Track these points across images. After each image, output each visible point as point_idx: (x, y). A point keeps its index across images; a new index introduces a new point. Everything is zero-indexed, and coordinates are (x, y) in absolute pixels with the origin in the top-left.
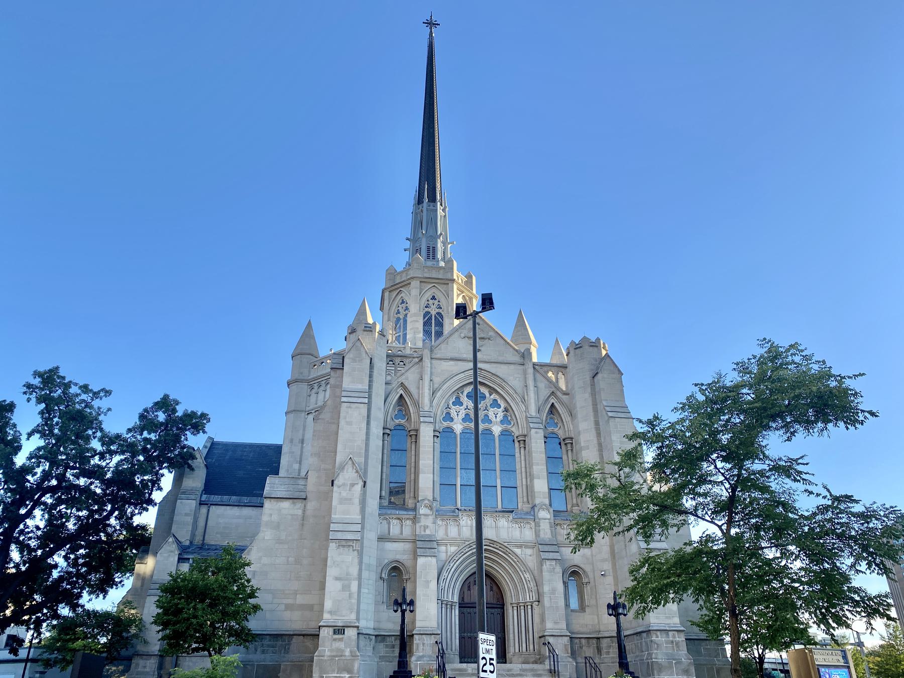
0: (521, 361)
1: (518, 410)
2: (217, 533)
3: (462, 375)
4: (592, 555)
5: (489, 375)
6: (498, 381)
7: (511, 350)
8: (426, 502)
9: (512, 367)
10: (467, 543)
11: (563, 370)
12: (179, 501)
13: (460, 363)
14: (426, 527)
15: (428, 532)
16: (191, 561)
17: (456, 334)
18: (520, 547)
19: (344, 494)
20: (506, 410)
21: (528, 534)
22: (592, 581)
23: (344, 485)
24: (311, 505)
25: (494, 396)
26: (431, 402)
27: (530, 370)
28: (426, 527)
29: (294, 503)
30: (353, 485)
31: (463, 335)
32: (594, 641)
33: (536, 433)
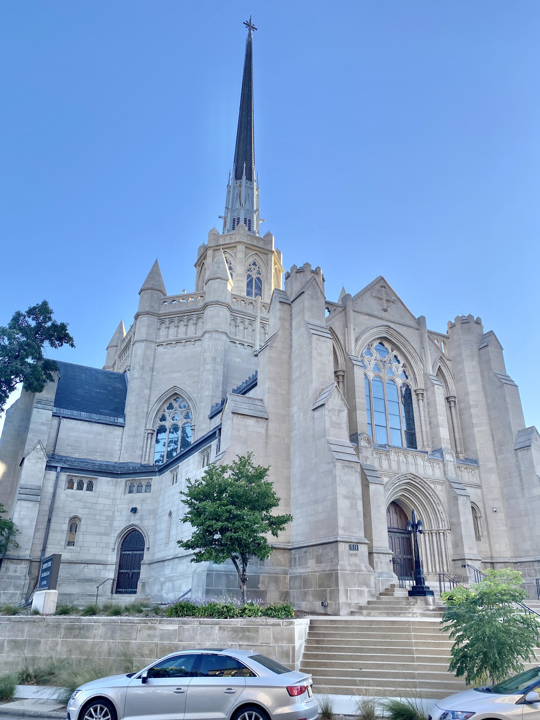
0: (417, 326)
1: (418, 368)
2: (67, 445)
3: (375, 330)
4: (483, 494)
5: (395, 334)
6: (402, 340)
7: (409, 315)
8: (365, 435)
9: (410, 329)
10: (398, 476)
11: (445, 340)
12: (35, 410)
13: (373, 319)
14: (367, 458)
15: (369, 463)
16: (59, 469)
17: (368, 293)
18: (434, 483)
19: (334, 418)
20: (404, 366)
21: (438, 473)
22: (483, 515)
23: (333, 409)
24: (272, 425)
25: (395, 353)
26: (355, 348)
27: (426, 335)
28: (367, 458)
29: (257, 421)
30: (340, 411)
31: (374, 295)
32: (489, 565)
33: (438, 389)
